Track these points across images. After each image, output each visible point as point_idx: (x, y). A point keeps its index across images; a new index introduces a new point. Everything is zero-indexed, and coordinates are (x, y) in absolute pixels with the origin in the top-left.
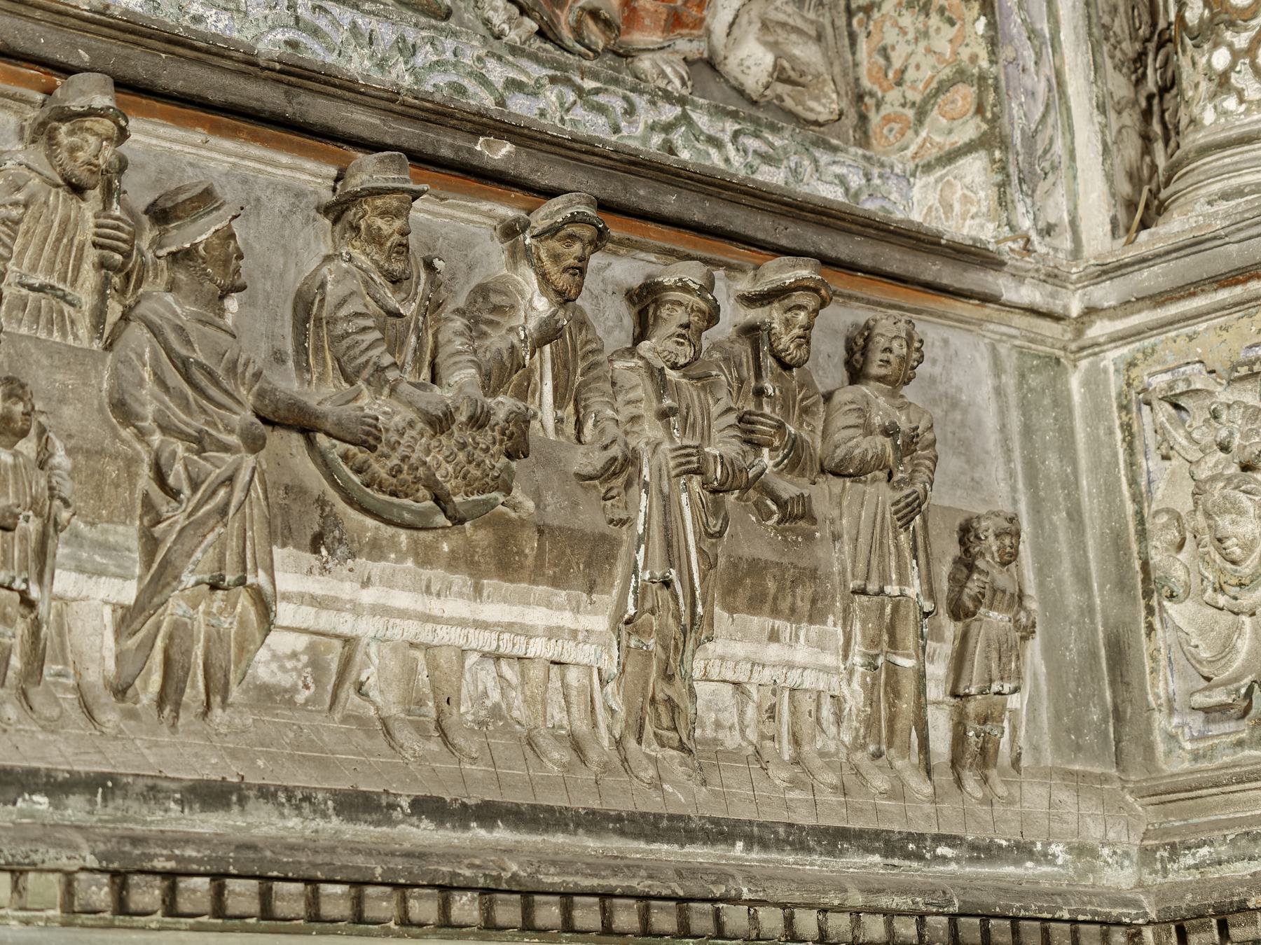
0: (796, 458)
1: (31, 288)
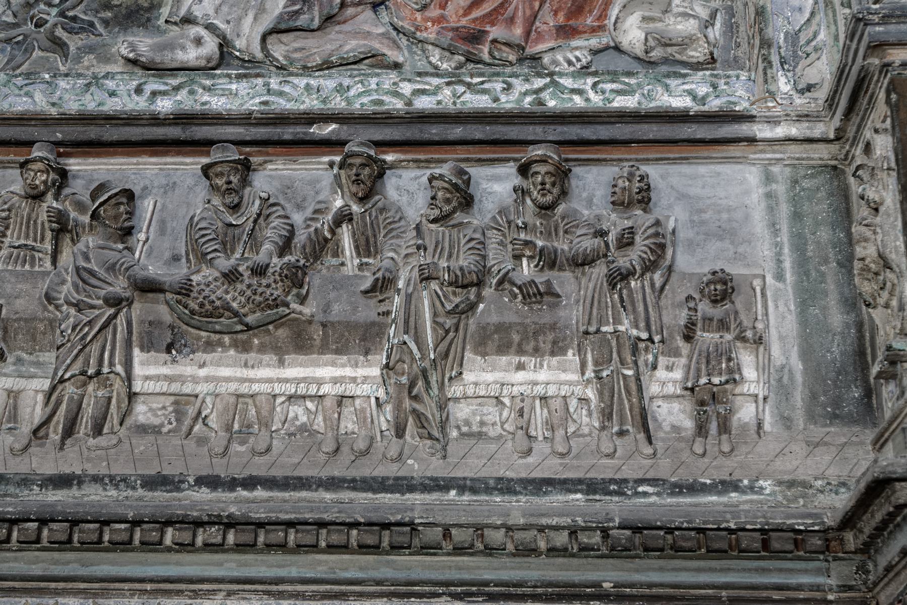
0: (549, 260)
1: (14, 247)
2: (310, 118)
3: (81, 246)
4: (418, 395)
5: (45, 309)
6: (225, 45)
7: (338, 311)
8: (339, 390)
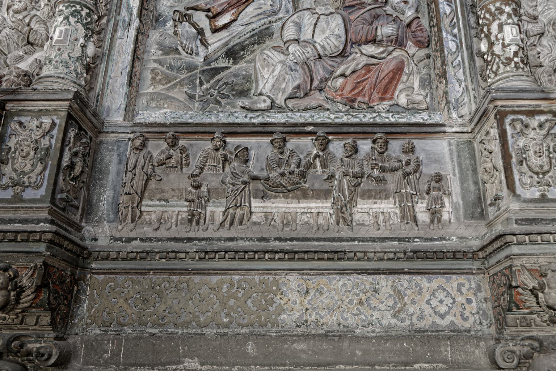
0: (383, 170)
2: (304, 125)
3: (232, 165)
4: (343, 212)
5: (222, 185)
6: (273, 102)
7: (317, 186)
8: (318, 210)
